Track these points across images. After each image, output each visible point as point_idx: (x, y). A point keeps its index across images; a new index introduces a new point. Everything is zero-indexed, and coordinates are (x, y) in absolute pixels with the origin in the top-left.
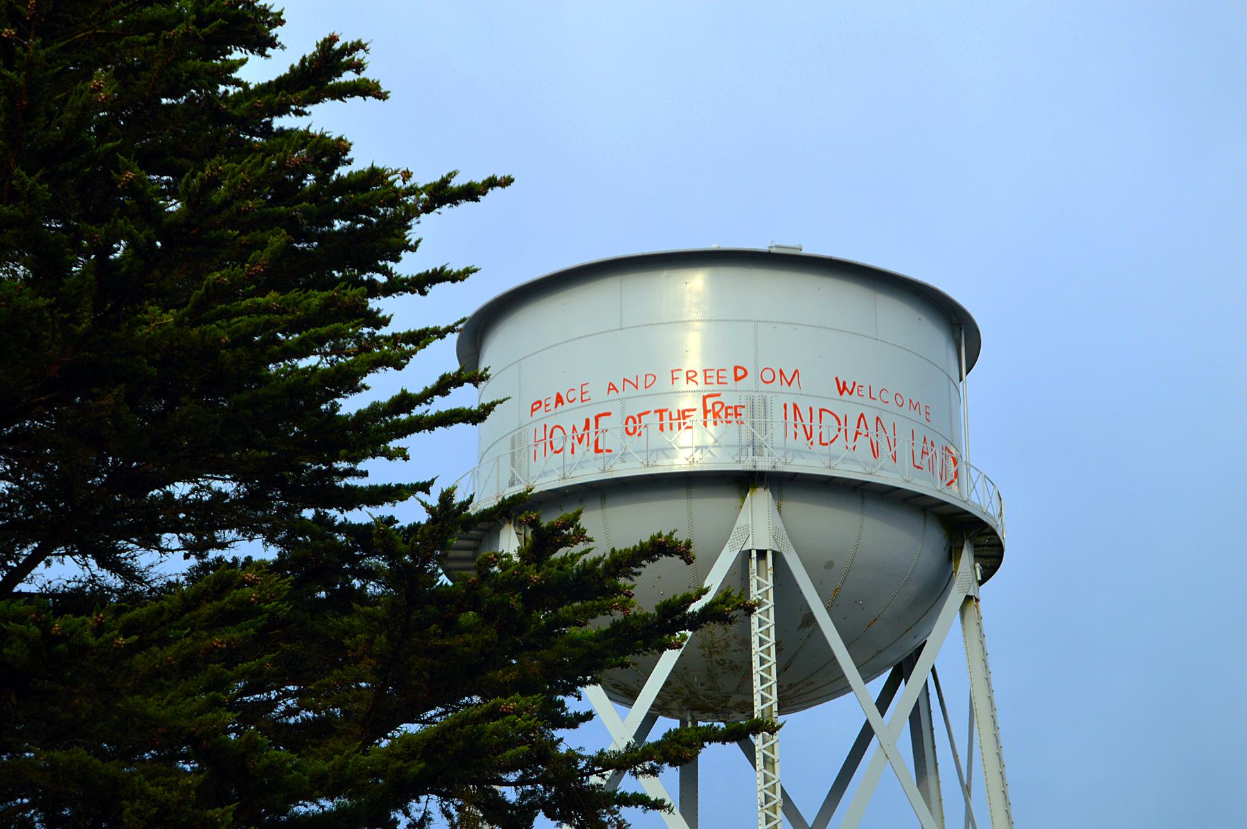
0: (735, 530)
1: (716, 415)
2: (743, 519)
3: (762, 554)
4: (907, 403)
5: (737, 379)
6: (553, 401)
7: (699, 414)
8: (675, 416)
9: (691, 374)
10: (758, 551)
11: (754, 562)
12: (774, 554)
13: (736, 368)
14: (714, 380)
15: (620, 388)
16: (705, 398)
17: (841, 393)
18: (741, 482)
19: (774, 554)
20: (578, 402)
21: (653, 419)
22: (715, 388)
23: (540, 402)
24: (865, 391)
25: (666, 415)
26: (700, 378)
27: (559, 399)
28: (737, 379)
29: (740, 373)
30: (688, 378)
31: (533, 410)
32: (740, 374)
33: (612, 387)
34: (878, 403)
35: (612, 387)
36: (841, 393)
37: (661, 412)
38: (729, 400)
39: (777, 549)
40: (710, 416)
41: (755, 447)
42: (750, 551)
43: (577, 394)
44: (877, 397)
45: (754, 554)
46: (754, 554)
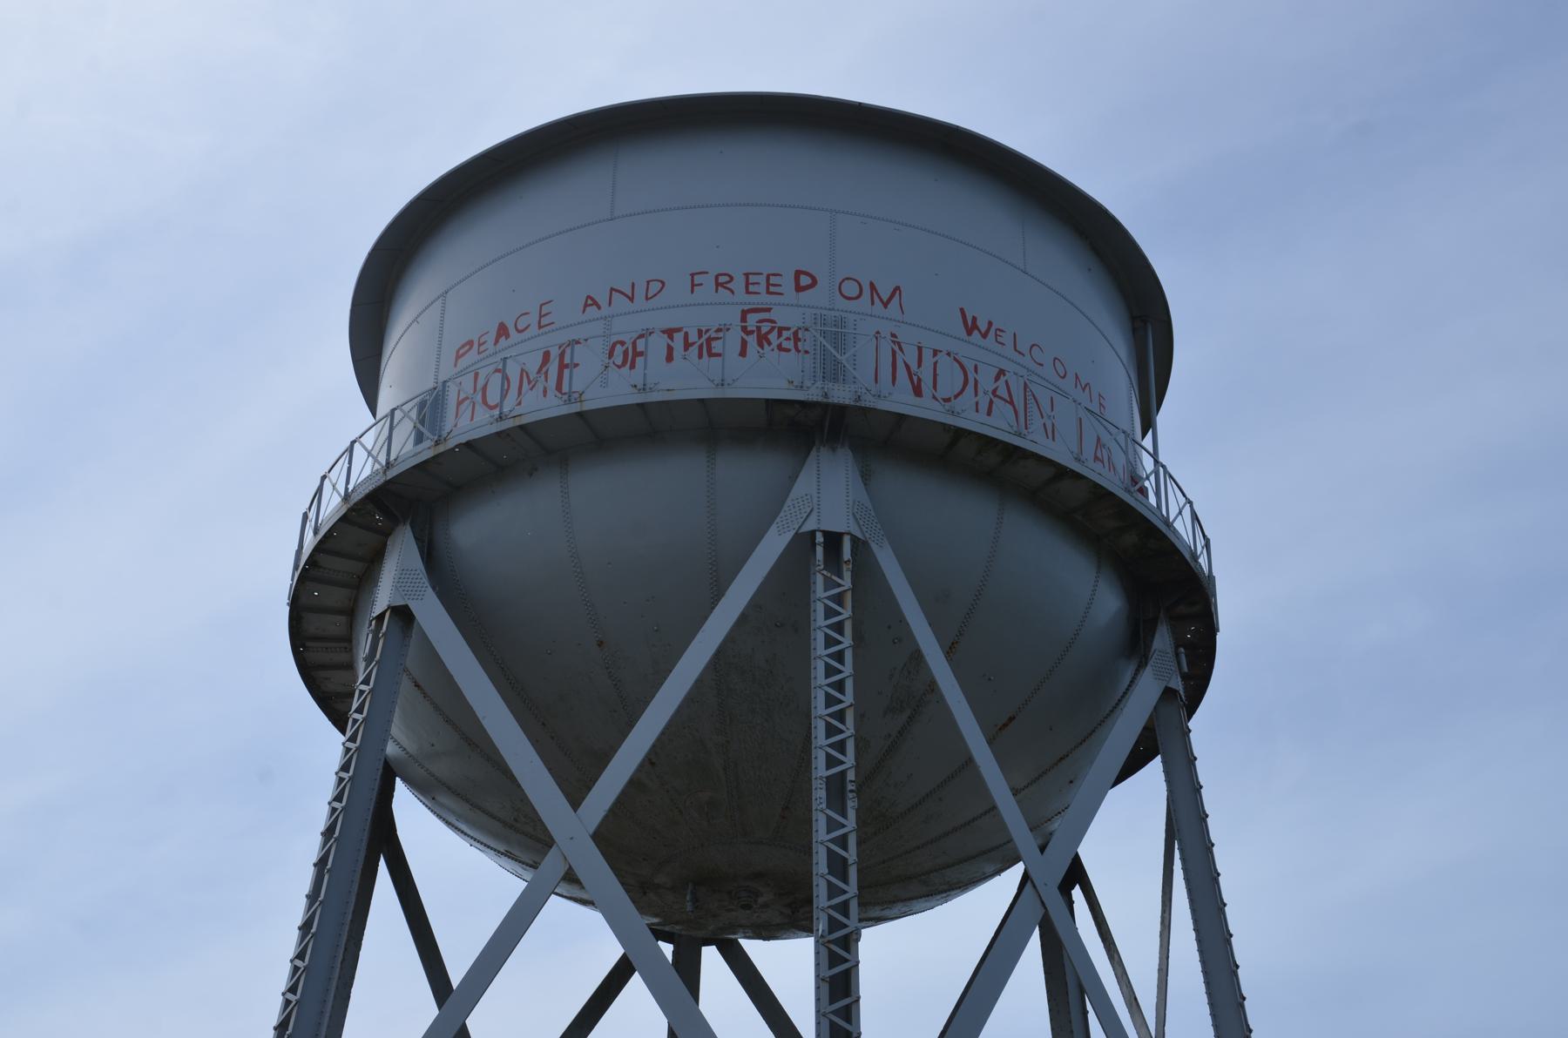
0: (789, 502)
1: (763, 340)
2: (805, 484)
3: (833, 540)
4: (1071, 378)
5: (799, 288)
6: (493, 335)
7: (735, 336)
8: (693, 337)
9: (722, 279)
10: (826, 534)
11: (820, 550)
12: (854, 540)
13: (798, 273)
14: (762, 288)
15: (603, 299)
16: (744, 314)
17: (969, 333)
18: (800, 428)
19: (854, 540)
20: (534, 330)
21: (658, 344)
22: (764, 299)
23: (470, 343)
24: (1007, 338)
25: (679, 337)
26: (738, 285)
27: (503, 331)
28: (799, 288)
29: (805, 280)
30: (718, 284)
31: (458, 357)
32: (804, 281)
33: (591, 302)
34: (1027, 360)
35: (591, 302)
36: (969, 333)
37: (670, 333)
38: (782, 316)
39: (859, 535)
40: (752, 340)
41: (834, 372)
42: (813, 533)
43: (533, 319)
44: (1026, 351)
45: (820, 538)
46: (820, 538)
